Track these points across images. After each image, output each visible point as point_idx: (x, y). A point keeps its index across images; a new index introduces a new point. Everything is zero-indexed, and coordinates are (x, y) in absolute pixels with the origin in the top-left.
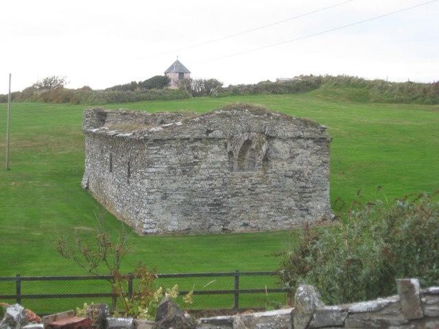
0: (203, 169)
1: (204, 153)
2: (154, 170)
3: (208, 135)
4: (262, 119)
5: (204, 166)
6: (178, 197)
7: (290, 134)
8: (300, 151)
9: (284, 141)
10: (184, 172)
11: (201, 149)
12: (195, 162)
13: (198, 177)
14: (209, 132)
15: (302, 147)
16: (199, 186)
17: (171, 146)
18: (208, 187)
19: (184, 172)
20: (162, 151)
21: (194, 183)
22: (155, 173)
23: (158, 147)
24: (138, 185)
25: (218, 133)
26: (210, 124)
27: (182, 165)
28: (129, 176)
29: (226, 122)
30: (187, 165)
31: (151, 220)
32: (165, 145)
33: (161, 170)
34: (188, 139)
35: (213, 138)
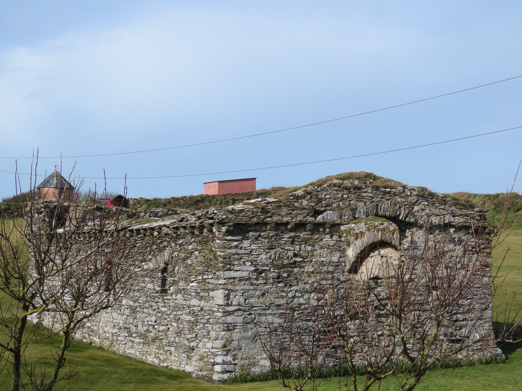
0: (309, 274)
1: (310, 248)
2: (233, 274)
3: (316, 218)
4: (395, 194)
5: (309, 268)
6: (270, 318)
7: (435, 220)
8: (451, 246)
9: (431, 229)
10: (278, 278)
11: (306, 241)
12: (295, 262)
13: (301, 286)
14: (317, 213)
15: (452, 241)
16: (302, 301)
17: (259, 236)
18: (315, 303)
19: (278, 278)
20: (246, 244)
21: (294, 297)
22: (234, 278)
23: (240, 238)
24: (194, 302)
25: (330, 216)
26: (320, 201)
27: (276, 267)
28: (164, 291)
29: (342, 199)
30: (284, 266)
31: (229, 358)
32: (251, 234)
33: (245, 274)
34: (287, 223)
35: (322, 225)
